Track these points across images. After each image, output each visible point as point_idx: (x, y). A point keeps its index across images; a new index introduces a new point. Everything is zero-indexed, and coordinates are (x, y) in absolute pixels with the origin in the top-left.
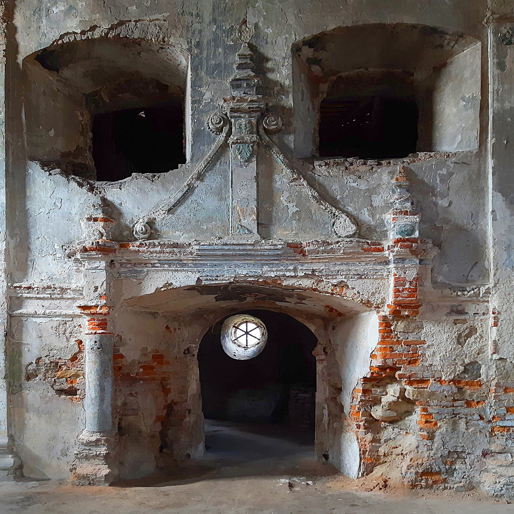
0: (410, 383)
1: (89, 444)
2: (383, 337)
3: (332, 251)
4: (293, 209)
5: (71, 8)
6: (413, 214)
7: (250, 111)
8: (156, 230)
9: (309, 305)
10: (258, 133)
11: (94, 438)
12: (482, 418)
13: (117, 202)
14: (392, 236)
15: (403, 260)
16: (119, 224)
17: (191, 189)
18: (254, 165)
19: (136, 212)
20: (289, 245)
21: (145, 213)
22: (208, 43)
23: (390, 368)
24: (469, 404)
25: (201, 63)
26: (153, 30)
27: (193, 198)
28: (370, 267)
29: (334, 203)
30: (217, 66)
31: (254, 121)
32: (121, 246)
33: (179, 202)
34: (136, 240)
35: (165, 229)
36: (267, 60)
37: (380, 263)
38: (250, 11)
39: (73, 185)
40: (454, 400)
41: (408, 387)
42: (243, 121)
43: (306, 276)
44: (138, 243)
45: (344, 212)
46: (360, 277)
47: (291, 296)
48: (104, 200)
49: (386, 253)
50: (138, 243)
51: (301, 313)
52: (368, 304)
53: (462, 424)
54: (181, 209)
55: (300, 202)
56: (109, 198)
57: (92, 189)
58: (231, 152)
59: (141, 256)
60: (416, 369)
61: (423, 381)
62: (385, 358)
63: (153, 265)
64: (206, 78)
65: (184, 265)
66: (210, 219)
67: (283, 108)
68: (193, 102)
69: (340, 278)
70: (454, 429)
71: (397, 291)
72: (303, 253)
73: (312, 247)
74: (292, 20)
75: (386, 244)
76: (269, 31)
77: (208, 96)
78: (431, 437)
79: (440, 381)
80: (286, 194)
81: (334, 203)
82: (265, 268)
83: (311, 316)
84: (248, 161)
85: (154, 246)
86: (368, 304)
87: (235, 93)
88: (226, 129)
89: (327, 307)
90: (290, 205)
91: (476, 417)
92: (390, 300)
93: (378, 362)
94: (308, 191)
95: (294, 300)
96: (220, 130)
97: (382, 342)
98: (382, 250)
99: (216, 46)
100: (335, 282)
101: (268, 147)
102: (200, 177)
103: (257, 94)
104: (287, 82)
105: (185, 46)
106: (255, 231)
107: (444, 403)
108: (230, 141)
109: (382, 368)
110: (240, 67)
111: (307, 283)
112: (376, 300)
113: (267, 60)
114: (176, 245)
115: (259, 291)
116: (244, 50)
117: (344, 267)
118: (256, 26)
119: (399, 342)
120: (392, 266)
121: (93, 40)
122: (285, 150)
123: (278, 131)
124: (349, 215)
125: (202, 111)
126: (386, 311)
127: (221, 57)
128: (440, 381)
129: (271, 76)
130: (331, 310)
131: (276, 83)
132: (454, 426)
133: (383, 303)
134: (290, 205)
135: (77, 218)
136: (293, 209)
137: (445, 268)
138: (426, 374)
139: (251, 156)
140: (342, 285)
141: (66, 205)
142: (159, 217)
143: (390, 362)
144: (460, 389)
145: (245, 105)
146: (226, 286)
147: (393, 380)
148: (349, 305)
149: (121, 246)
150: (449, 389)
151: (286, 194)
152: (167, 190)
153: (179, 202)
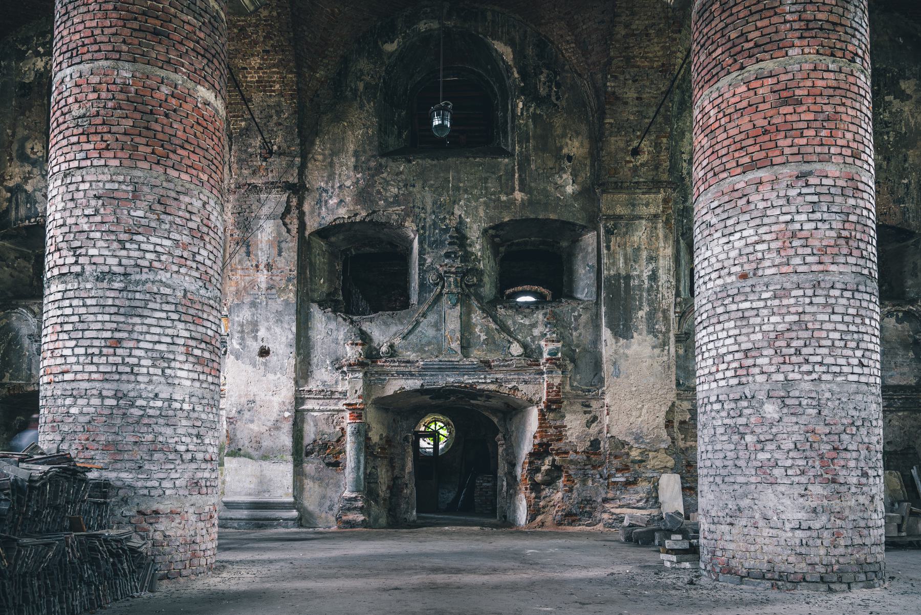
0: (557, 454)
1: (350, 499)
2: (540, 424)
3: (509, 366)
4: (483, 337)
5: (341, 201)
6: (558, 342)
7: (455, 273)
8: (395, 351)
9: (493, 402)
10: (461, 286)
11: (354, 495)
12: (601, 477)
13: (369, 331)
14: (546, 356)
15: (552, 372)
16: (370, 346)
17: (418, 323)
18: (458, 308)
19: (381, 338)
20: (481, 361)
21: (387, 339)
22: (430, 226)
23: (544, 444)
24: (594, 467)
25: (425, 239)
26: (394, 217)
27: (419, 329)
28: (532, 376)
29: (509, 333)
30: (435, 241)
31: (459, 279)
32: (373, 362)
33: (410, 332)
34: (381, 357)
35: (400, 350)
36: (467, 239)
37: (538, 374)
38: (456, 206)
39: (340, 319)
40: (585, 465)
41: (557, 458)
42: (452, 279)
43: (492, 382)
44: (383, 360)
45: (516, 339)
46: (526, 382)
47: (481, 396)
48: (360, 330)
49: (542, 367)
50: (383, 360)
51: (487, 408)
52: (531, 402)
53: (590, 483)
54: (411, 337)
55: (488, 331)
56: (364, 329)
57: (352, 322)
58: (445, 298)
59: (385, 368)
60: (561, 444)
61: (567, 453)
62: (542, 437)
63: (393, 375)
64: (429, 250)
65: (412, 375)
66: (429, 343)
67: (477, 270)
68: (420, 265)
69: (514, 384)
70: (585, 485)
71: (548, 392)
72: (490, 367)
73: (496, 363)
74: (482, 214)
75: (542, 361)
76: (468, 220)
77: (429, 260)
78: (571, 490)
79: (576, 452)
80: (479, 327)
81: (509, 333)
82: (466, 377)
83: (495, 411)
84: (455, 305)
85: (394, 362)
86: (531, 402)
87: (447, 261)
88: (441, 284)
89: (506, 403)
90: (482, 334)
91: (598, 476)
92: (544, 399)
93: (537, 441)
94: (493, 326)
95: (483, 399)
96: (437, 284)
97: (540, 427)
98: (539, 365)
99: (435, 229)
100: (510, 386)
101: (468, 296)
102: (424, 315)
103: (461, 262)
104: (479, 254)
105: (415, 228)
106: (459, 352)
107: (579, 467)
108: (444, 292)
109: (540, 445)
110: (450, 244)
111: (492, 387)
112: (536, 398)
113: (467, 239)
114: (408, 362)
115: (460, 392)
116: (452, 232)
117: (516, 377)
118: (460, 216)
119: (550, 427)
120: (545, 376)
121: (355, 222)
122: (480, 298)
123: (474, 285)
124: (518, 341)
125: (425, 271)
126: (542, 406)
127: (438, 236)
128: (576, 452)
129: (469, 249)
130: (507, 405)
131: (472, 254)
132: (584, 482)
133: (541, 399)
134: (482, 334)
135: (342, 343)
136: (483, 337)
137: (578, 377)
138: (568, 448)
139: (457, 302)
140: (515, 389)
141: (335, 333)
142: (397, 341)
143: (545, 440)
144: (588, 457)
145: (453, 270)
146: (440, 389)
147: (547, 453)
148: (520, 402)
149: (373, 362)
150: (581, 457)
151: (479, 327)
152: (402, 323)
153: (410, 332)
